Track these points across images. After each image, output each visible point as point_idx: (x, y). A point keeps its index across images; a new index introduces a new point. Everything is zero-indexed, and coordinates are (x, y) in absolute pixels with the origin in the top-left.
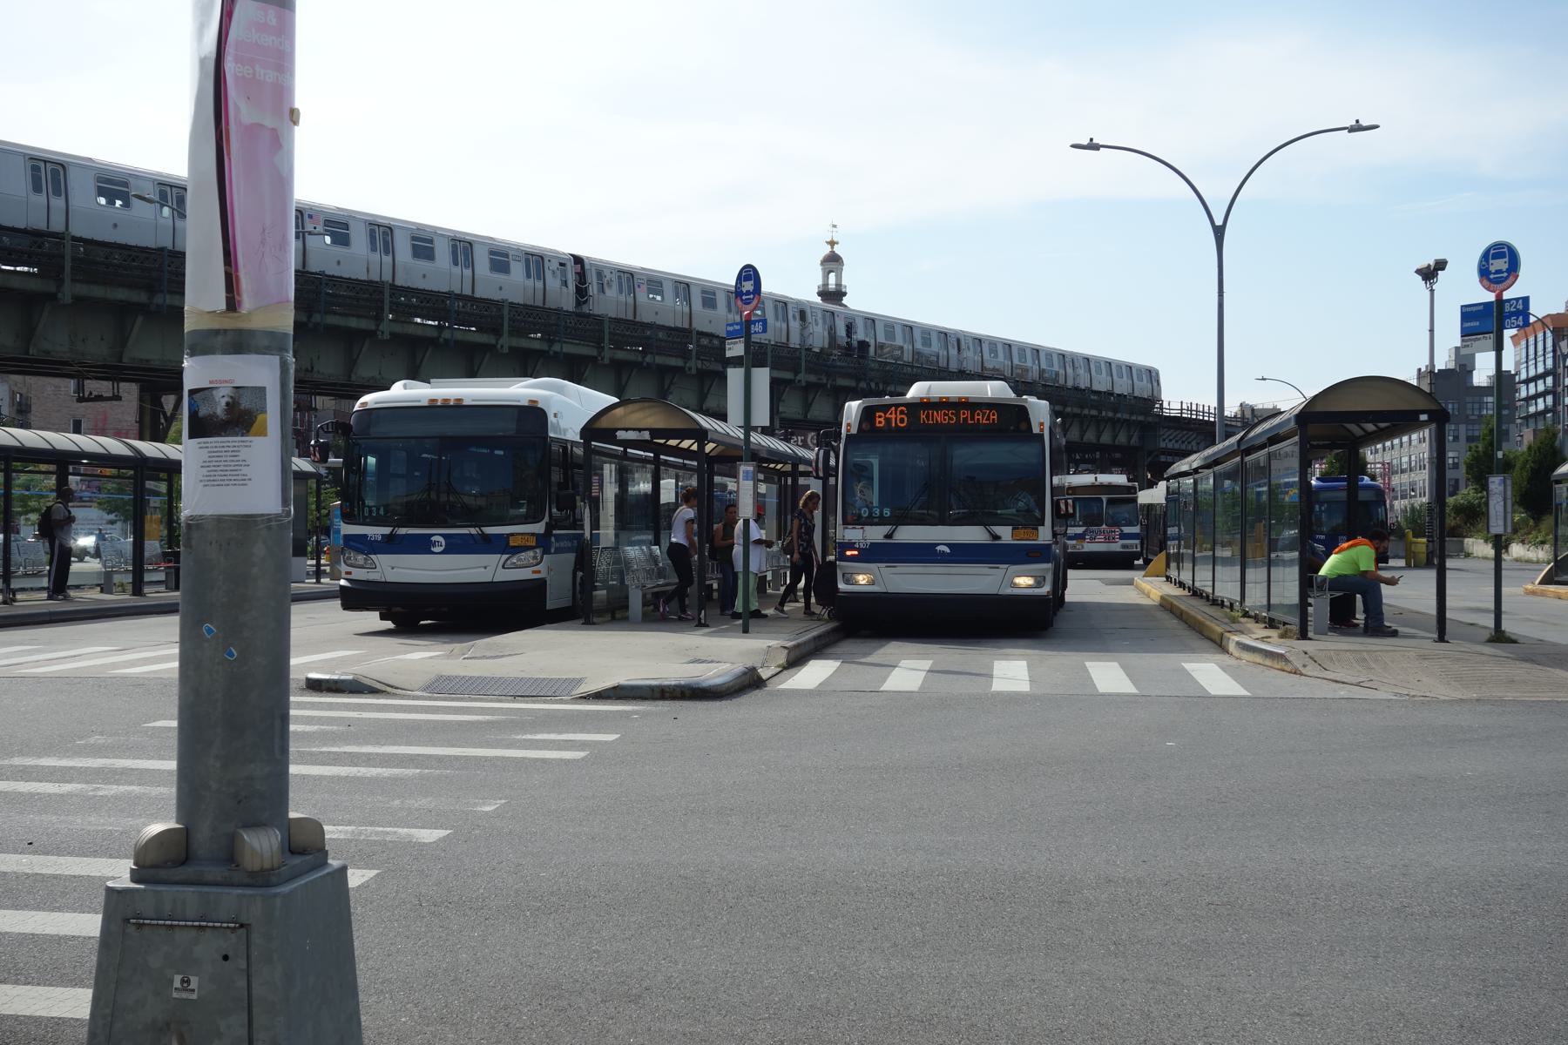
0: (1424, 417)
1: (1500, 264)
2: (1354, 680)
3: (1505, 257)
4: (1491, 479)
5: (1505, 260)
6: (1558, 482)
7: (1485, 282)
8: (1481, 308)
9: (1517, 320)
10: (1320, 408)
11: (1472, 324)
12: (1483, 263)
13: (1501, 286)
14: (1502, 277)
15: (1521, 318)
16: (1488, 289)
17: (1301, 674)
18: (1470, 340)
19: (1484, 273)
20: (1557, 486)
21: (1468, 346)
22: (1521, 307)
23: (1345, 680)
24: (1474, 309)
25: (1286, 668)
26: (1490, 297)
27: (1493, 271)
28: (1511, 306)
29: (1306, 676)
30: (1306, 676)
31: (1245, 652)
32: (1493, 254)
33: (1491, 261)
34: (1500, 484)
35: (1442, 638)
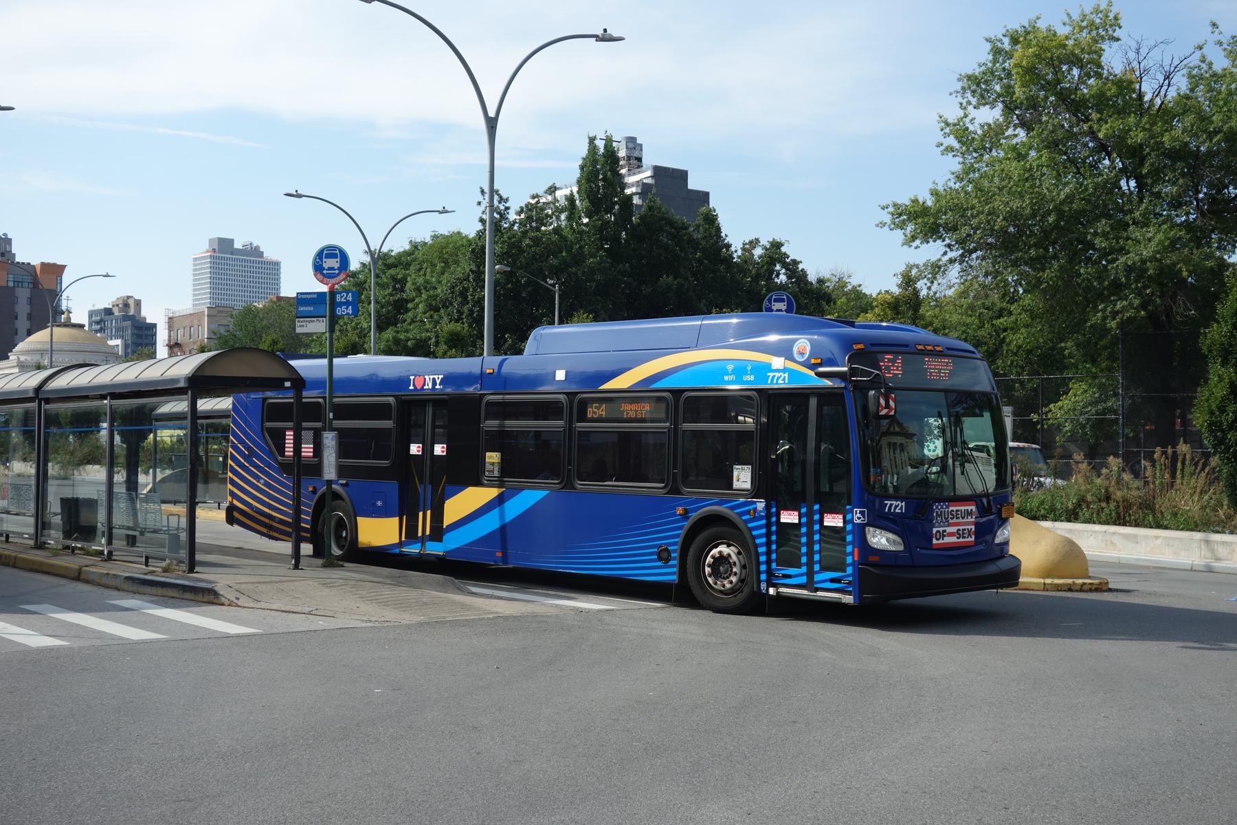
0: (288, 384)
1: (333, 263)
2: (307, 610)
3: (337, 258)
4: (325, 435)
5: (337, 260)
6: (157, 420)
7: (319, 276)
8: (315, 296)
9: (347, 309)
10: (208, 373)
11: (307, 309)
12: (318, 260)
13: (334, 281)
14: (335, 273)
15: (350, 307)
16: (322, 282)
17: (239, 606)
18: (307, 321)
19: (318, 268)
20: (156, 423)
21: (303, 326)
22: (350, 299)
23: (294, 610)
24: (309, 296)
25: (215, 601)
26: (324, 288)
27: (326, 268)
28: (341, 297)
29: (241, 607)
30: (241, 607)
31: (142, 586)
32: (326, 254)
33: (324, 260)
34: (332, 440)
35: (296, 567)
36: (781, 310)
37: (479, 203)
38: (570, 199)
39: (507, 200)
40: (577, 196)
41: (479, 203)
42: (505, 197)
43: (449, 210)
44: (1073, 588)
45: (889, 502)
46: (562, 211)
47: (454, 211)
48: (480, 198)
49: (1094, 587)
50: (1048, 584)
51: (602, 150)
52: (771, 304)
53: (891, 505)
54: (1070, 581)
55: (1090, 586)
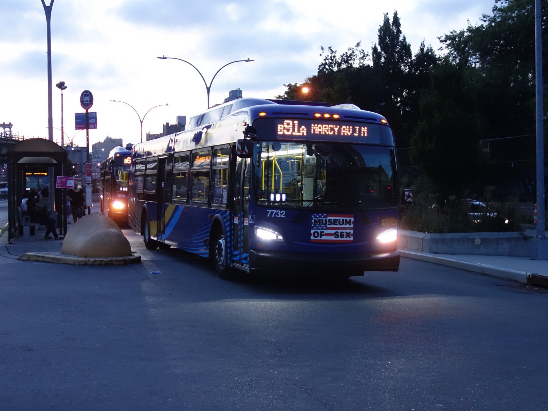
36: (87, 101)
37: (321, 55)
38: (375, 49)
39: (336, 52)
40: (379, 48)
41: (321, 55)
42: (334, 50)
43: (251, 60)
44: (87, 263)
45: (270, 211)
46: (368, 55)
47: (254, 60)
48: (321, 52)
49: (103, 263)
50: (75, 260)
51: (391, 21)
52: (83, 98)
53: (272, 213)
54: (87, 259)
55: (99, 263)
